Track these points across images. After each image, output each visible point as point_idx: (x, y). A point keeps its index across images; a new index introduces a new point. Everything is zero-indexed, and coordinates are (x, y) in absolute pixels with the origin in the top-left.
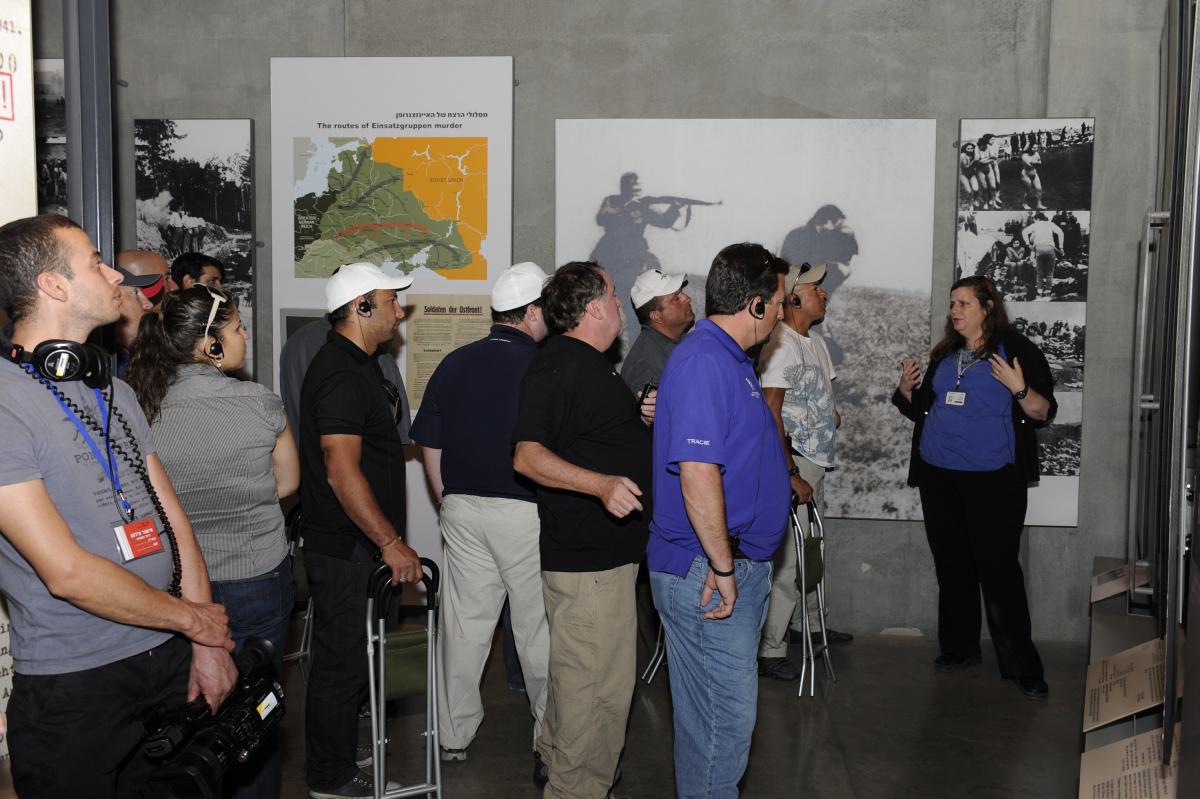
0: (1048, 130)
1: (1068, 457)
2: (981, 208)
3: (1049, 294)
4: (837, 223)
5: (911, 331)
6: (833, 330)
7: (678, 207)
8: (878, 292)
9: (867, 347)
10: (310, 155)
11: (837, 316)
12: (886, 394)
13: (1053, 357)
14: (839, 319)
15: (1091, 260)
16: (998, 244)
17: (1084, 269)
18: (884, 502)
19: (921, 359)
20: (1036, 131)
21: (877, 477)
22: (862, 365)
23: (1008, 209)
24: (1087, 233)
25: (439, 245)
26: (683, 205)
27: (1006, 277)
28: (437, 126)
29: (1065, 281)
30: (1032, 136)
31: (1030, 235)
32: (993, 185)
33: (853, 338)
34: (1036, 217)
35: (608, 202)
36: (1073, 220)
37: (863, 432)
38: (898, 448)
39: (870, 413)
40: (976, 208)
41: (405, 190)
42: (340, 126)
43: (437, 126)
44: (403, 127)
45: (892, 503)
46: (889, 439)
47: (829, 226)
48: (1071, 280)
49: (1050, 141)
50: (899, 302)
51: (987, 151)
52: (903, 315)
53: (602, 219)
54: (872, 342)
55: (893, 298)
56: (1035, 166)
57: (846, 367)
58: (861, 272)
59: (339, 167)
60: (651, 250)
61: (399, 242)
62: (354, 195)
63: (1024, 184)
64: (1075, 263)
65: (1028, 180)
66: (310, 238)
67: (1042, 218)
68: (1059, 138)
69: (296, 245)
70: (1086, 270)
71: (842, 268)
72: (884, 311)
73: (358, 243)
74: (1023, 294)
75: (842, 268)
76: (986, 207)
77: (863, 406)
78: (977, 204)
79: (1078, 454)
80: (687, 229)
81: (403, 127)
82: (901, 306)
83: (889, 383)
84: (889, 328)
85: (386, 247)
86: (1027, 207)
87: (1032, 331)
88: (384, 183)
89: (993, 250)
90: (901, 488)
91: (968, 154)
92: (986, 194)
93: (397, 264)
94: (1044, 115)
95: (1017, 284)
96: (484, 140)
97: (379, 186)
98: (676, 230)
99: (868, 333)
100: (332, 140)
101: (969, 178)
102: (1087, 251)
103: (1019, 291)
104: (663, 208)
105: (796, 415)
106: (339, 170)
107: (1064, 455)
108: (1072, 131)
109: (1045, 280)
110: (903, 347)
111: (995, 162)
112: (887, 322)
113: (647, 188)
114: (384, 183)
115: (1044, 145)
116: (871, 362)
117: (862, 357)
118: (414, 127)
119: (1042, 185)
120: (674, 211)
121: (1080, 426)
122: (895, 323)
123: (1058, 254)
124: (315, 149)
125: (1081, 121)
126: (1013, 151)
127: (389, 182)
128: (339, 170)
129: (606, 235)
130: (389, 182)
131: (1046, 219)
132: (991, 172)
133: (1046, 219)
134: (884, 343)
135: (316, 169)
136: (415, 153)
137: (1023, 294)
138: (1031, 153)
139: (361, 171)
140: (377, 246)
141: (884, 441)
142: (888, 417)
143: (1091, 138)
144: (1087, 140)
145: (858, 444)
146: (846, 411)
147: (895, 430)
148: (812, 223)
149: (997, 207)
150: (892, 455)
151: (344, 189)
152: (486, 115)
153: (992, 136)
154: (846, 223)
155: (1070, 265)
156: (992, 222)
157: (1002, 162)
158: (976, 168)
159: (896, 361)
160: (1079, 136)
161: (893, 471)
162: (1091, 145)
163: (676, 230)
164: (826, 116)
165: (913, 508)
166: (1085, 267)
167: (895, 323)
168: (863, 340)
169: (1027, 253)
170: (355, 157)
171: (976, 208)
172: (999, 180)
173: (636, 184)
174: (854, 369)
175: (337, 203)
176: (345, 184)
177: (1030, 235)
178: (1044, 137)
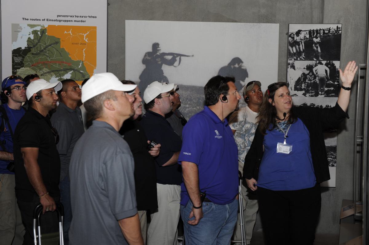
0: (323, 29)
1: (332, 159)
2: (297, 60)
3: (324, 94)
4: (240, 65)
7: (176, 57)
10: (19, 32)
16: (304, 74)
23: (307, 60)
25: (76, 71)
26: (178, 57)
27: (307, 87)
28: (75, 21)
29: (330, 89)
30: (317, 31)
31: (316, 70)
32: (302, 50)
34: (318, 63)
35: (147, 54)
36: (333, 65)
40: (295, 60)
41: (61, 47)
42: (32, 20)
43: (75, 21)
44: (60, 21)
47: (237, 66)
48: (332, 89)
49: (324, 33)
51: (299, 36)
53: (144, 61)
56: (318, 43)
59: (32, 37)
60: (165, 74)
61: (59, 69)
62: (39, 49)
63: (314, 50)
64: (334, 82)
65: (315, 48)
66: (18, 67)
67: (321, 64)
68: (328, 32)
69: (13, 69)
73: (40, 69)
74: (313, 94)
76: (299, 59)
78: (295, 58)
79: (336, 158)
80: (179, 66)
81: (60, 21)
85: (53, 71)
86: (315, 59)
88: (52, 44)
91: (292, 38)
92: (298, 54)
93: (58, 78)
94: (322, 22)
95: (311, 90)
96: (95, 28)
97: (50, 45)
100: (29, 25)
101: (292, 47)
103: (312, 93)
104: (170, 57)
105: (239, 141)
106: (32, 38)
107: (330, 159)
108: (333, 29)
109: (322, 88)
111: (303, 41)
113: (163, 49)
114: (52, 44)
115: (322, 34)
118: (65, 21)
119: (321, 51)
120: (174, 58)
121: (336, 147)
123: (327, 78)
124: (21, 29)
125: (336, 25)
126: (309, 37)
127: (54, 44)
128: (32, 38)
129: (146, 68)
130: (54, 44)
131: (322, 64)
132: (301, 45)
133: (322, 64)
135: (22, 38)
136: (66, 32)
137: (313, 94)
138: (317, 38)
139: (42, 39)
140: (49, 71)
143: (340, 32)
144: (339, 32)
148: (230, 64)
149: (303, 59)
151: (34, 46)
152: (96, 17)
153: (301, 31)
154: (243, 65)
155: (332, 82)
156: (301, 65)
157: (305, 41)
158: (295, 43)
160: (336, 31)
162: (340, 35)
164: (236, 22)
169: (315, 77)
170: (39, 33)
171: (295, 60)
172: (304, 49)
173: (159, 47)
175: (31, 52)
176: (35, 44)
177: (316, 70)
178: (322, 31)
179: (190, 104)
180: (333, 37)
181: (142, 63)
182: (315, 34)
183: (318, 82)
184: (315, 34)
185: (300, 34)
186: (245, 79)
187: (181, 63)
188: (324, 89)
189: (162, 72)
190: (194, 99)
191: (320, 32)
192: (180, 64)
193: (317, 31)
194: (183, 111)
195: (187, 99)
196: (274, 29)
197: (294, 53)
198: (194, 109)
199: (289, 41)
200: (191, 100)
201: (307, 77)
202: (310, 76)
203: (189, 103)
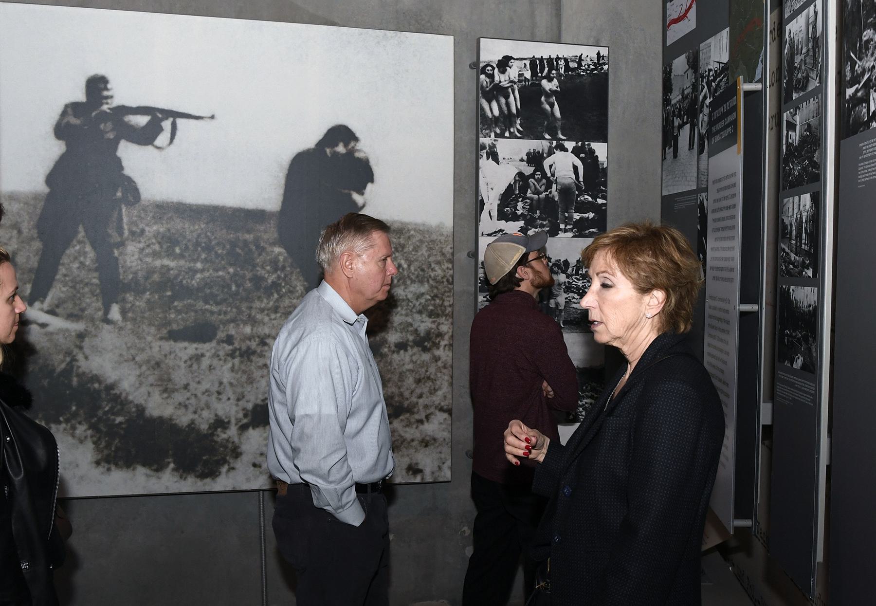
2: (501, 136)
3: (571, 230)
5: (433, 270)
7: (162, 120)
12: (408, 340)
13: (576, 296)
15: (609, 195)
16: (520, 174)
17: (603, 204)
18: (409, 462)
19: (443, 301)
20: (554, 56)
21: (400, 436)
24: (605, 166)
26: (167, 119)
27: (529, 211)
29: (586, 215)
30: (550, 60)
31: (551, 166)
32: (514, 111)
34: (557, 147)
35: (69, 110)
36: (592, 152)
38: (421, 401)
39: (391, 363)
45: (417, 464)
46: (412, 392)
47: (341, 149)
48: (591, 215)
50: (419, 237)
51: (507, 73)
52: (424, 251)
53: (61, 131)
55: (412, 232)
56: (553, 92)
60: (127, 172)
64: (595, 197)
70: (605, 205)
71: (356, 197)
72: (403, 247)
75: (356, 197)
76: (507, 134)
78: (498, 131)
80: (172, 146)
82: (421, 241)
83: (411, 329)
84: (409, 266)
86: (547, 136)
87: (556, 269)
89: (516, 181)
90: (426, 446)
92: (505, 121)
94: (557, 40)
95: (540, 218)
102: (606, 187)
103: (542, 226)
104: (142, 120)
108: (588, 60)
109: (566, 215)
110: (425, 288)
111: (515, 86)
112: (406, 260)
113: (122, 93)
115: (562, 71)
122: (416, 260)
123: (578, 188)
126: (532, 76)
131: (566, 150)
132: (512, 96)
133: (566, 150)
134: (404, 283)
138: (550, 80)
141: (407, 394)
142: (410, 367)
143: (606, 67)
144: (602, 69)
147: (418, 381)
148: (322, 144)
149: (519, 135)
150: (416, 410)
153: (511, 58)
154: (359, 146)
155: (590, 199)
156: (514, 150)
158: (496, 92)
159: (418, 304)
160: (595, 64)
161: (417, 428)
162: (606, 74)
165: (440, 468)
166: (604, 202)
167: (416, 260)
169: (549, 186)
171: (497, 135)
173: (107, 89)
177: (551, 166)
178: (562, 63)
179: (205, 261)
180: (589, 79)
181: (53, 135)
182: (547, 69)
183: (556, 199)
184: (547, 69)
185: (508, 68)
186: (365, 188)
187: (176, 137)
188: (572, 217)
189: (118, 163)
190: (218, 244)
191: (557, 64)
192: (177, 140)
193: (552, 63)
194: (184, 282)
195: (197, 244)
196: (439, 49)
197: (493, 116)
198: (221, 273)
199: (482, 86)
200: (208, 249)
201: (529, 184)
202: (536, 180)
203: (203, 256)
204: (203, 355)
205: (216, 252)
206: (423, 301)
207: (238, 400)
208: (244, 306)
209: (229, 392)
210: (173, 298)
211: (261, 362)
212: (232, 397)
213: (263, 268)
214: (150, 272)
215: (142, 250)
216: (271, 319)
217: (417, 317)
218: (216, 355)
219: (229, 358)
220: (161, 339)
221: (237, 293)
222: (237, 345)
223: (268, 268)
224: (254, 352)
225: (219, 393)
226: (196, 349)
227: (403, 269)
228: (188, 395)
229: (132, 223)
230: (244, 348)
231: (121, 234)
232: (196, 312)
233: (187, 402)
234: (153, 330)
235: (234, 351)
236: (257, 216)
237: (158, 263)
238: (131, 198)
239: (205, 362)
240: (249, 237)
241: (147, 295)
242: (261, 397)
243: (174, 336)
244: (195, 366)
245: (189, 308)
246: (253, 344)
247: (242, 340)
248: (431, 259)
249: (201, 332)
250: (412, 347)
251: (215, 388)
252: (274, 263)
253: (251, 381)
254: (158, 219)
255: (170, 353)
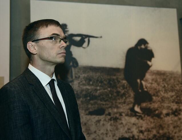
5: (176, 87)
6: (148, 88)
8: (163, 72)
9: (161, 94)
11: (148, 82)
14: (150, 83)
22: (159, 101)
33: (155, 91)
37: (163, 129)
38: (176, 135)
47: (143, 47)
52: (172, 81)
54: (162, 92)
55: (168, 74)
57: (154, 102)
58: (158, 64)
75: (149, 63)
77: (161, 118)
80: (88, 47)
82: (171, 77)
84: (168, 86)
98: (84, 48)
99: (161, 88)
110: (173, 94)
112: (167, 84)
116: (163, 100)
117: (159, 98)
134: (167, 92)
141: (171, 132)
142: (171, 122)
145: (162, 134)
146: (156, 121)
147: (174, 127)
163: (84, 48)
168: (159, 91)
174: (156, 103)
179: (100, 86)
190: (105, 80)
195: (97, 80)
198: (106, 90)
200: (101, 82)
203: (100, 84)
204: (100, 120)
205: (104, 83)
206: (173, 98)
207: (113, 136)
208: (114, 102)
209: (110, 134)
210: (90, 100)
211: (120, 122)
212: (111, 135)
213: (120, 88)
214: (82, 91)
215: (79, 83)
216: (123, 106)
217: (172, 104)
218: (105, 120)
219: (109, 121)
220: (87, 114)
221: (111, 97)
222: (112, 116)
223: (121, 88)
224: (118, 118)
225: (107, 134)
226: (98, 118)
227: (166, 87)
228: (96, 135)
229: (76, 74)
230: (114, 117)
231: (72, 77)
232: (98, 104)
233: (96, 138)
234: (83, 111)
235: (111, 118)
236: (117, 70)
237: (85, 87)
238: (75, 65)
239: (102, 123)
240: (115, 77)
241: (81, 99)
242: (121, 135)
243: (91, 113)
244: (98, 124)
245: (95, 103)
246: (118, 116)
247: (114, 114)
248: (175, 83)
249: (100, 112)
250: (171, 115)
251: (105, 132)
252: (124, 87)
253: (117, 129)
254: (84, 72)
255: (90, 120)
